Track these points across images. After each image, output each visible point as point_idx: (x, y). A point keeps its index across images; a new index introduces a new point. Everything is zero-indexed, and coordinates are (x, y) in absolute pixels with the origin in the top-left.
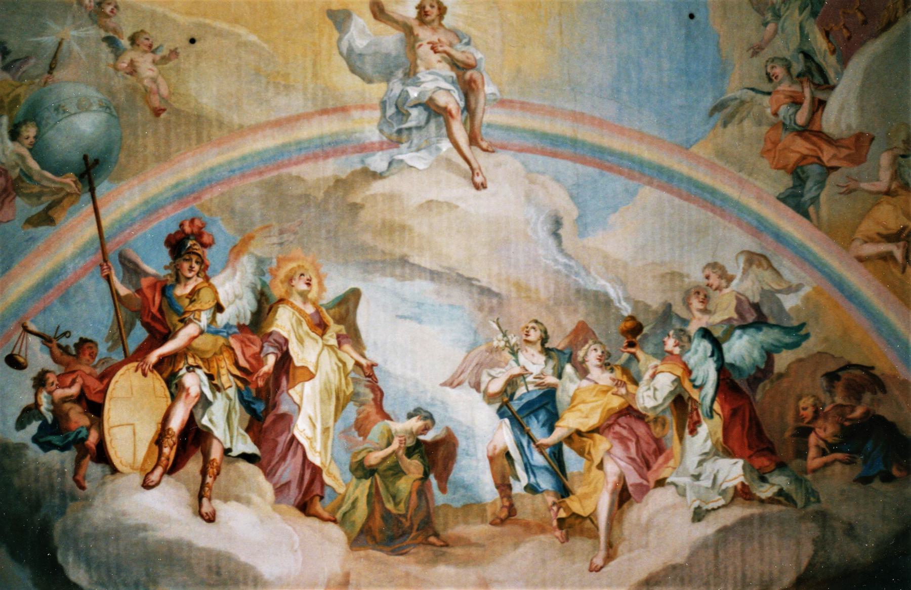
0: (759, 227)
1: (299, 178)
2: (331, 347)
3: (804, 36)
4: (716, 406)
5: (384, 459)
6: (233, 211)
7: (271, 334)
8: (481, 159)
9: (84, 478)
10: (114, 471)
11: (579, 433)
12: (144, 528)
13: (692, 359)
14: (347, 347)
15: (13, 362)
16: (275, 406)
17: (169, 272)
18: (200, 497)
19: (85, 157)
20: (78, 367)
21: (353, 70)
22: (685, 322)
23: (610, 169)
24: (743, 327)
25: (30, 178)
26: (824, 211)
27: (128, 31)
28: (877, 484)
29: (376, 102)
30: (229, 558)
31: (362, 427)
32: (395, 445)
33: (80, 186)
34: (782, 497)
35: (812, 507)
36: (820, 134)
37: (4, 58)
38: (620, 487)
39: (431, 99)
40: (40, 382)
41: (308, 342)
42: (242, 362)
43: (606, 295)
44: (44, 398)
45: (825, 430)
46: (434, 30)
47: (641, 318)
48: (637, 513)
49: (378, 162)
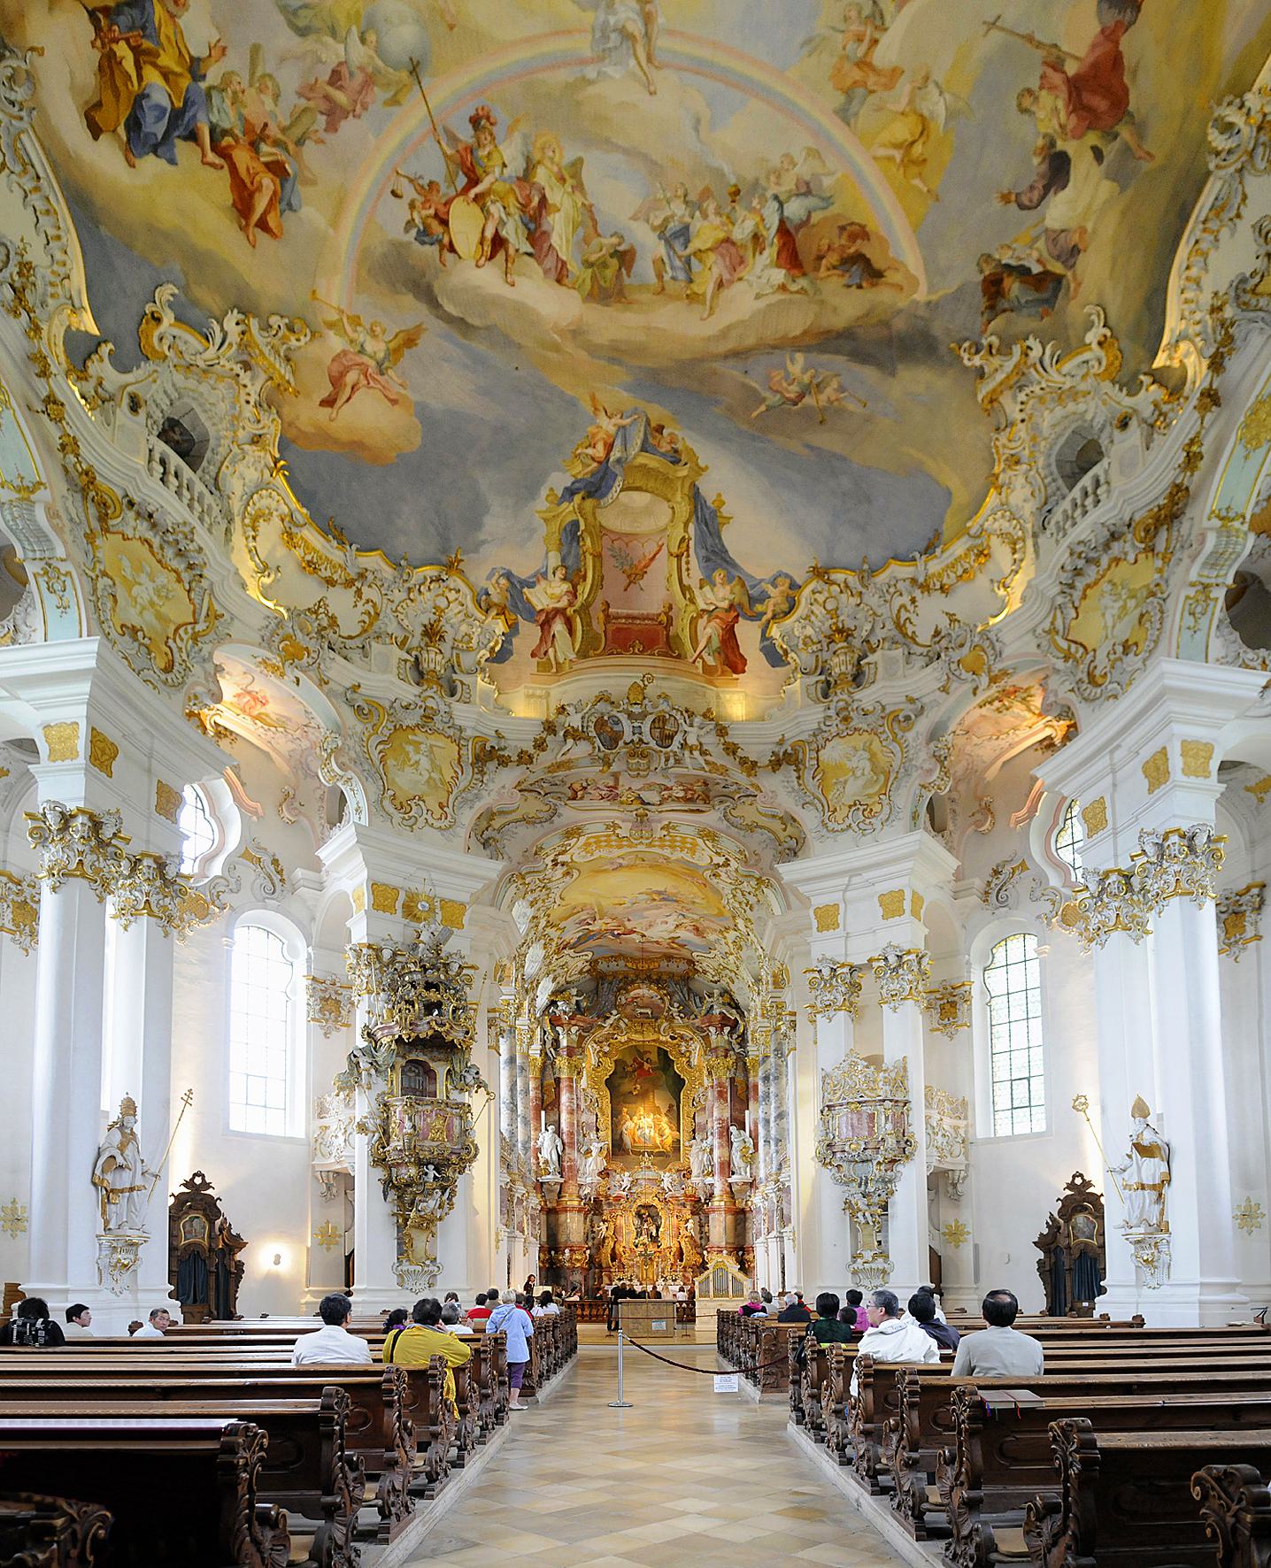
8: (656, 75)
24: (797, 195)
34: (802, 291)
35: (817, 297)
36: (870, 66)
49: (591, 72)
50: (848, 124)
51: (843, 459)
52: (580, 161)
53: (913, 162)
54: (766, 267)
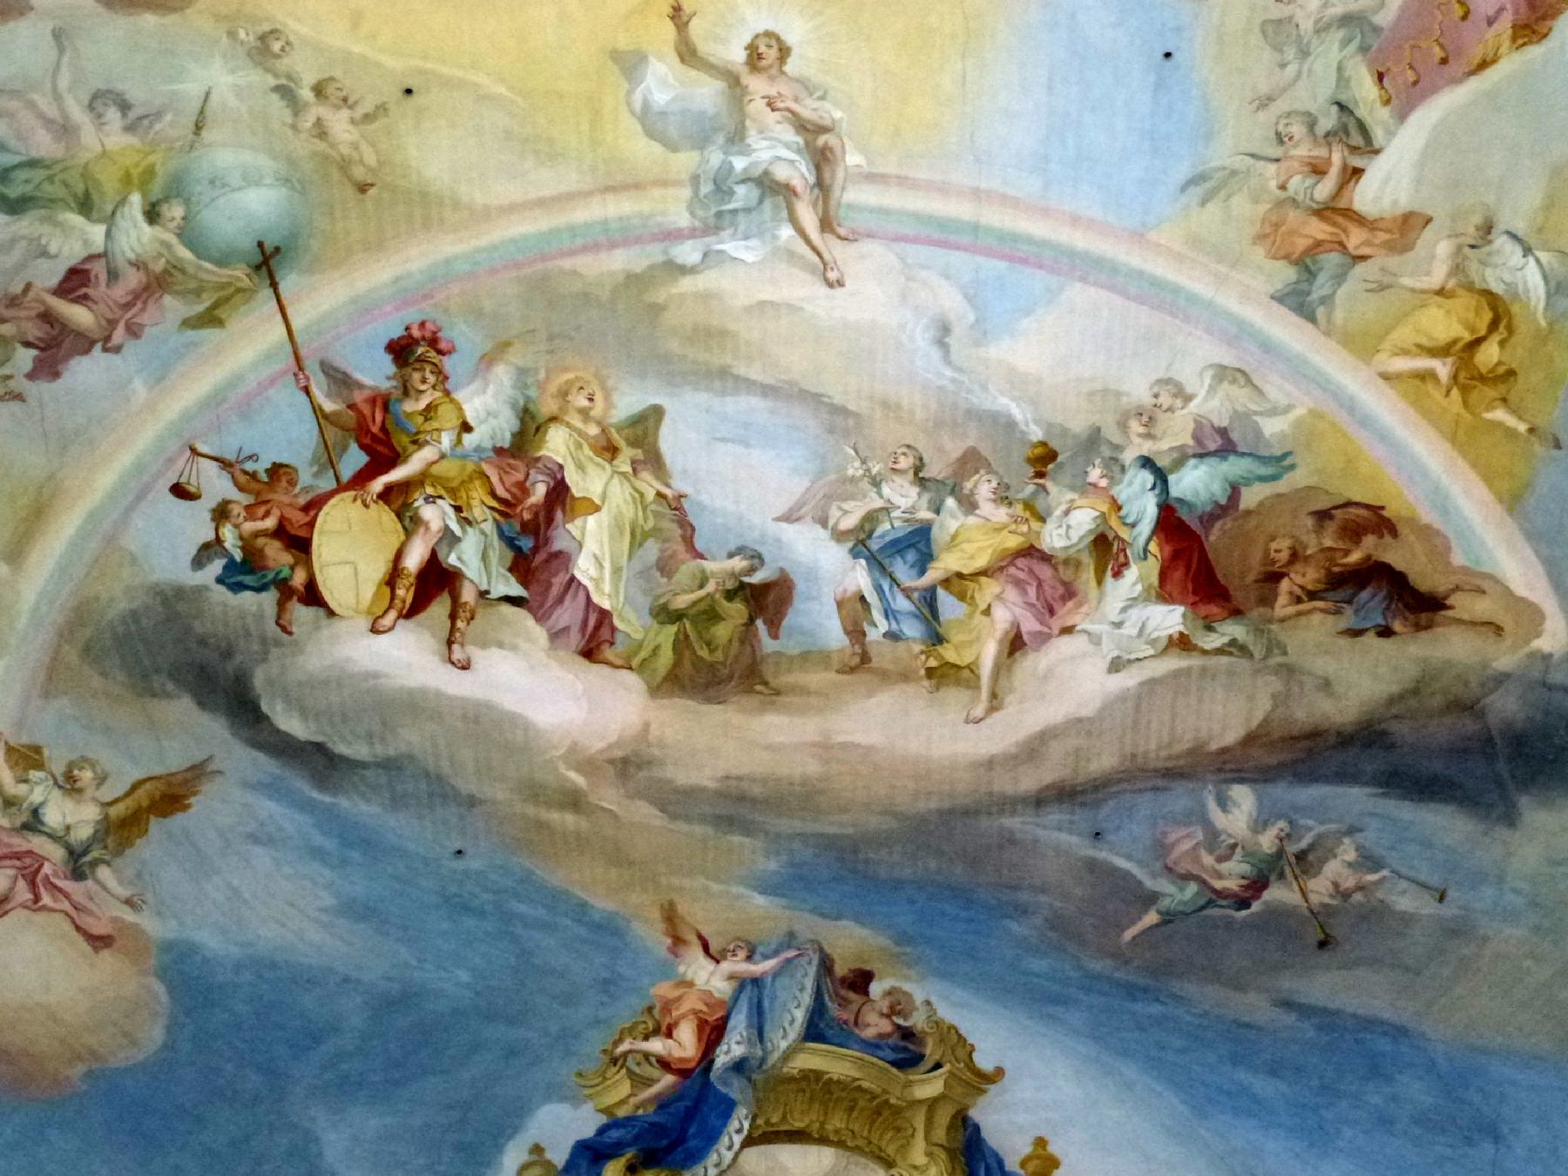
0: (1238, 333)
1: (574, 273)
2: (623, 474)
3: (1342, 79)
4: (1153, 547)
5: (695, 603)
6: (479, 313)
7: (538, 459)
8: (835, 250)
9: (291, 624)
10: (331, 613)
11: (960, 575)
12: (376, 675)
13: (1123, 493)
14: (646, 475)
15: (179, 491)
16: (547, 541)
17: (394, 383)
18: (450, 643)
19: (260, 245)
20: (271, 496)
21: (651, 134)
22: (1118, 448)
23: (1024, 261)
24: (1201, 456)
25: (183, 271)
26: (1339, 316)
27: (309, 78)
28: (1371, 639)
29: (685, 176)
30: (489, 706)
31: (665, 567)
32: (710, 587)
33: (256, 280)
34: (1234, 648)
37: (124, 115)
38: (1012, 635)
39: (766, 173)
40: (221, 513)
41: (591, 469)
42: (501, 492)
43: (1010, 416)
44: (229, 535)
45: (1304, 575)
46: (772, 79)
47: (1054, 444)
48: (1032, 664)
49: (688, 253)
50: (1312, 319)
51: (1398, 1032)
52: (657, 412)
53: (1482, 379)
54: (1133, 602)
